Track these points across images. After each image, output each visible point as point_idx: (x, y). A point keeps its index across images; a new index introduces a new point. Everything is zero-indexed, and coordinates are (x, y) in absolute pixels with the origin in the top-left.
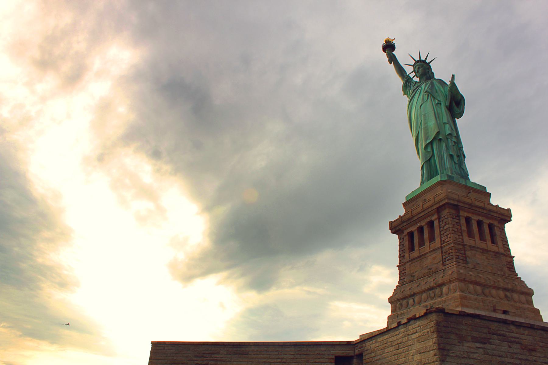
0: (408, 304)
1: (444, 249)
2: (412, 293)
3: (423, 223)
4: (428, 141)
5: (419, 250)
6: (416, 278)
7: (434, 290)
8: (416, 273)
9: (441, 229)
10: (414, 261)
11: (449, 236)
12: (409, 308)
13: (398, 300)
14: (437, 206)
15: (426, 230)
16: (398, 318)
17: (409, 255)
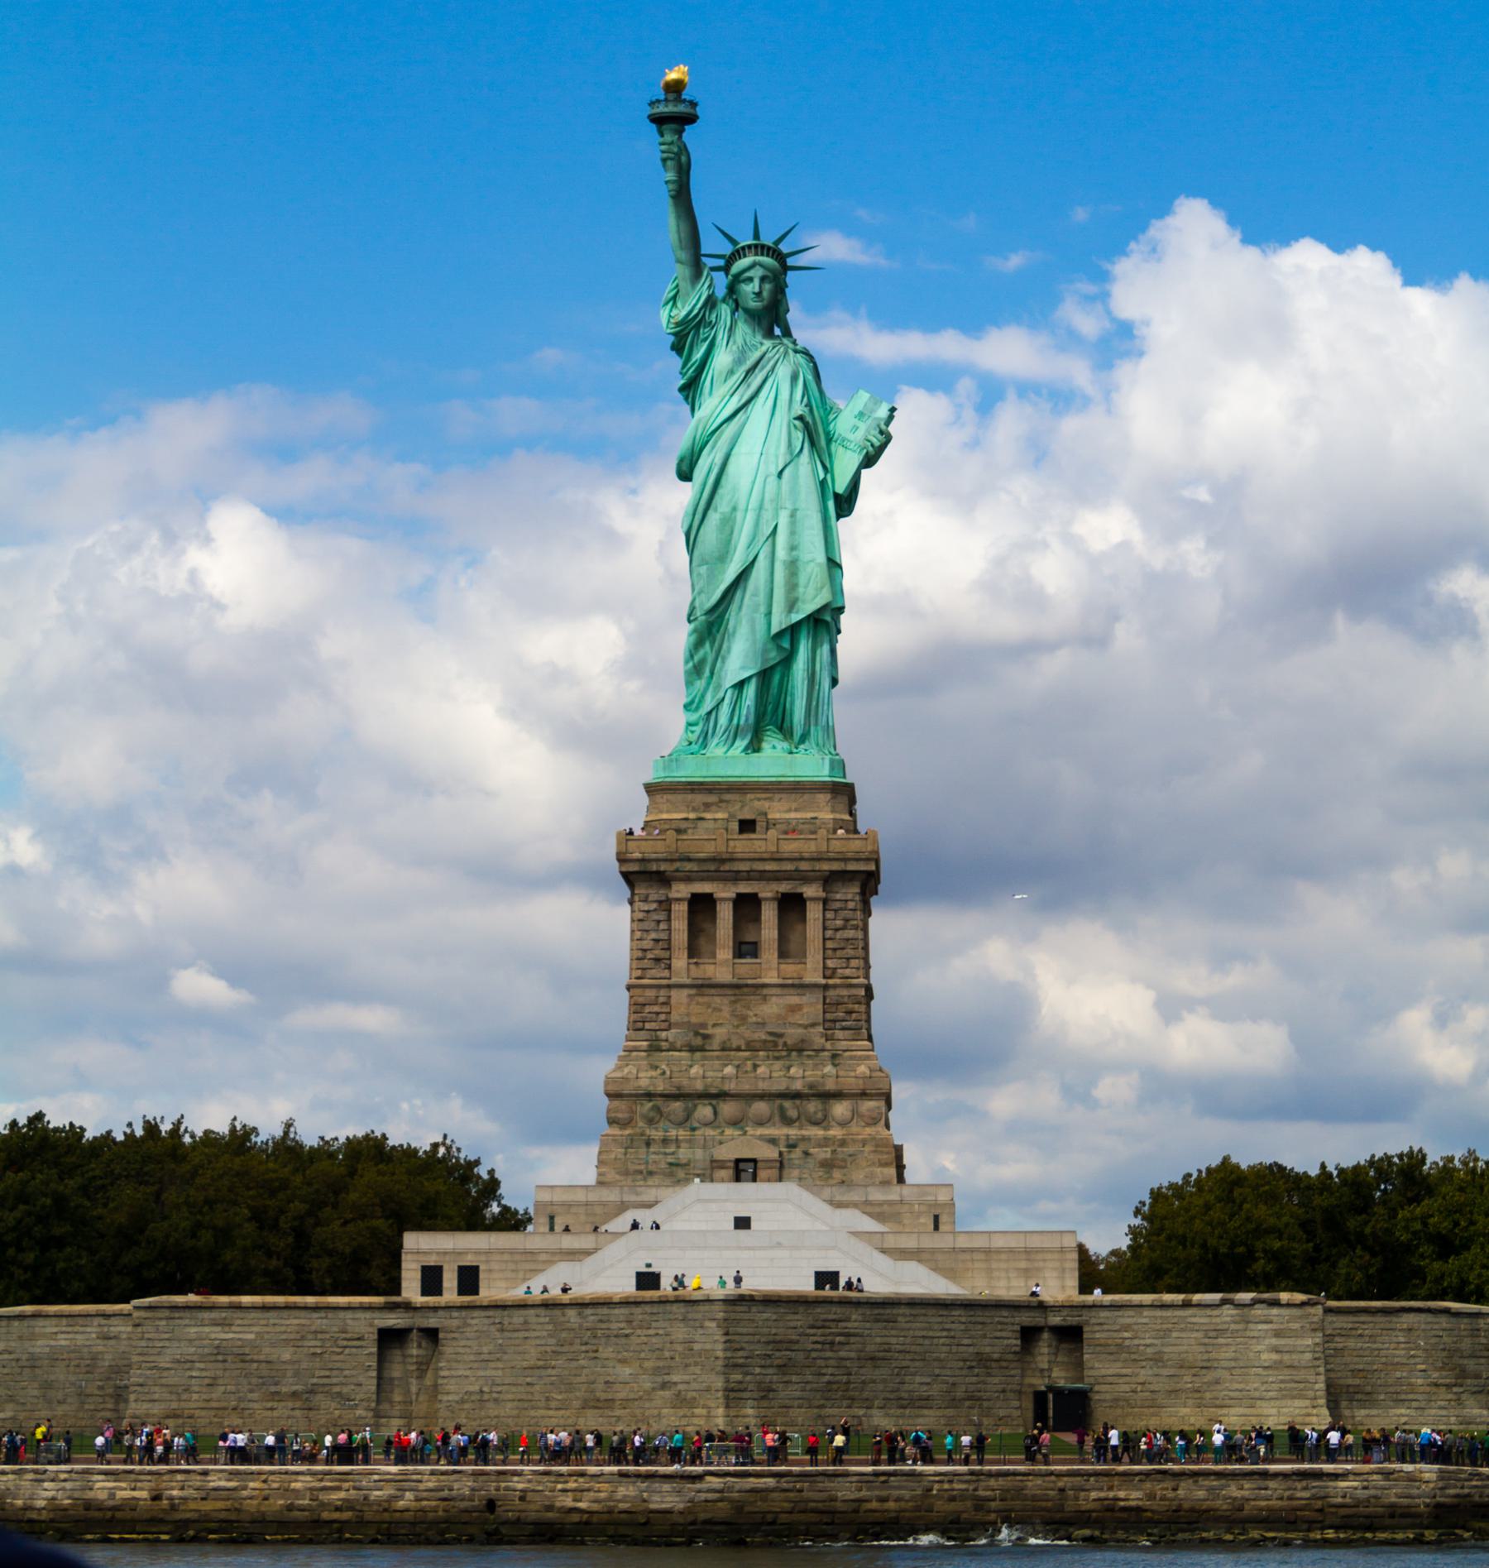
0: (688, 1118)
1: (831, 993)
2: (713, 1091)
3: (766, 891)
4: (796, 617)
5: (734, 964)
6: (716, 1047)
7: (798, 1102)
9: (829, 933)
10: (713, 991)
11: (854, 963)
12: (693, 1129)
13: (649, 1096)
14: (836, 866)
15: (769, 914)
17: (689, 964)
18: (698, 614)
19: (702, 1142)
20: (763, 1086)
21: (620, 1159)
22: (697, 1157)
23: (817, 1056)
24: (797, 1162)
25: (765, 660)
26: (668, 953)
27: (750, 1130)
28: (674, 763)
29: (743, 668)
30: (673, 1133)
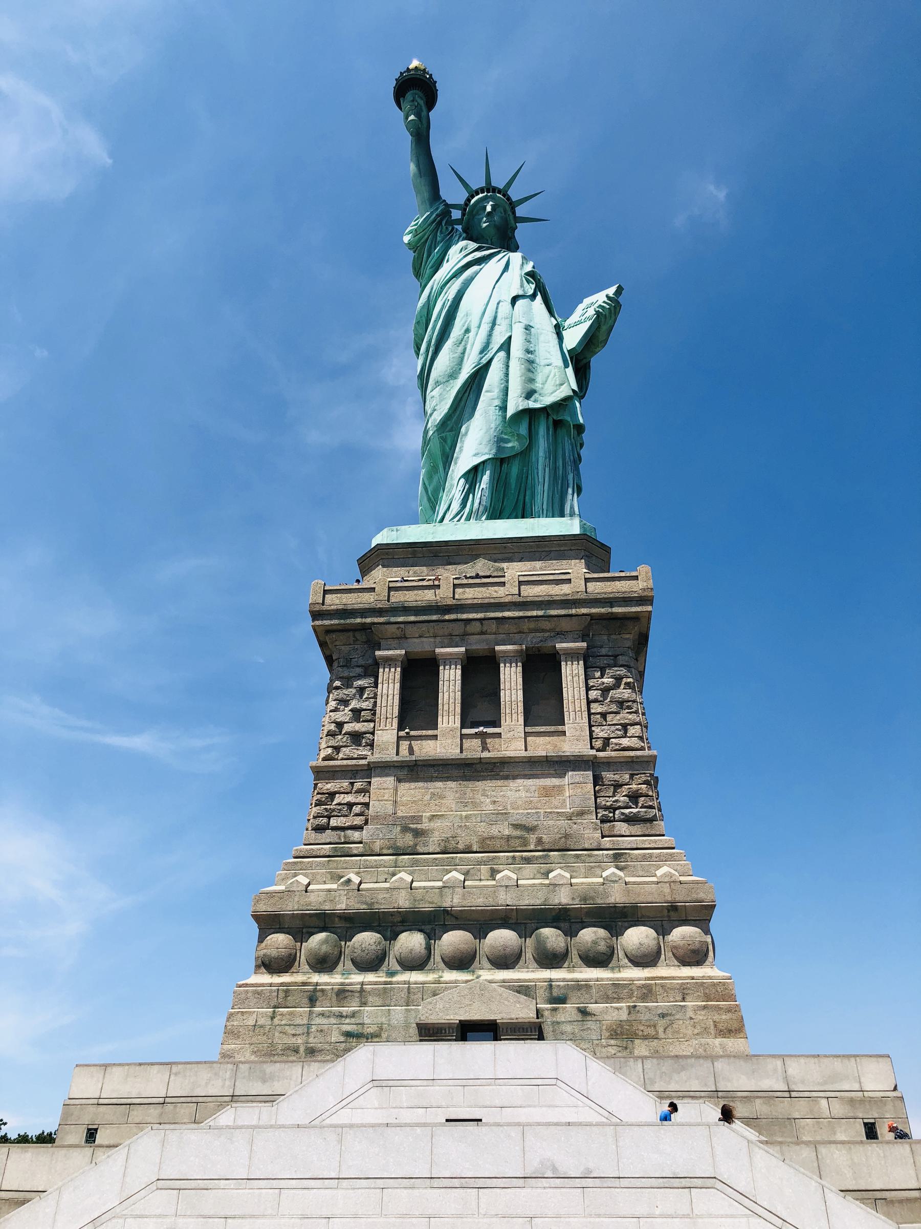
2: (426, 907)
4: (532, 404)
8: (437, 824)
9: (593, 694)
12: (392, 974)
16: (313, 1006)
17: (399, 738)
18: (431, 433)
19: (406, 990)
20: (506, 899)
21: (261, 1027)
22: (395, 1022)
23: (589, 856)
24: (568, 1028)
25: (499, 449)
26: (372, 725)
27: (488, 975)
28: (395, 532)
29: (476, 455)
30: (357, 978)
